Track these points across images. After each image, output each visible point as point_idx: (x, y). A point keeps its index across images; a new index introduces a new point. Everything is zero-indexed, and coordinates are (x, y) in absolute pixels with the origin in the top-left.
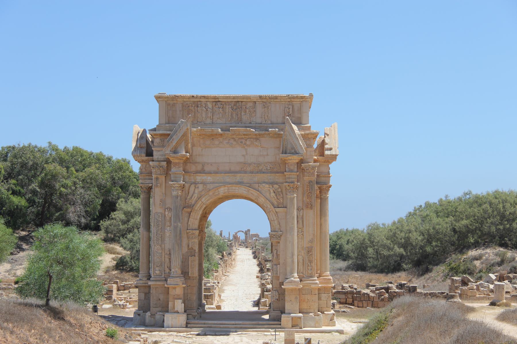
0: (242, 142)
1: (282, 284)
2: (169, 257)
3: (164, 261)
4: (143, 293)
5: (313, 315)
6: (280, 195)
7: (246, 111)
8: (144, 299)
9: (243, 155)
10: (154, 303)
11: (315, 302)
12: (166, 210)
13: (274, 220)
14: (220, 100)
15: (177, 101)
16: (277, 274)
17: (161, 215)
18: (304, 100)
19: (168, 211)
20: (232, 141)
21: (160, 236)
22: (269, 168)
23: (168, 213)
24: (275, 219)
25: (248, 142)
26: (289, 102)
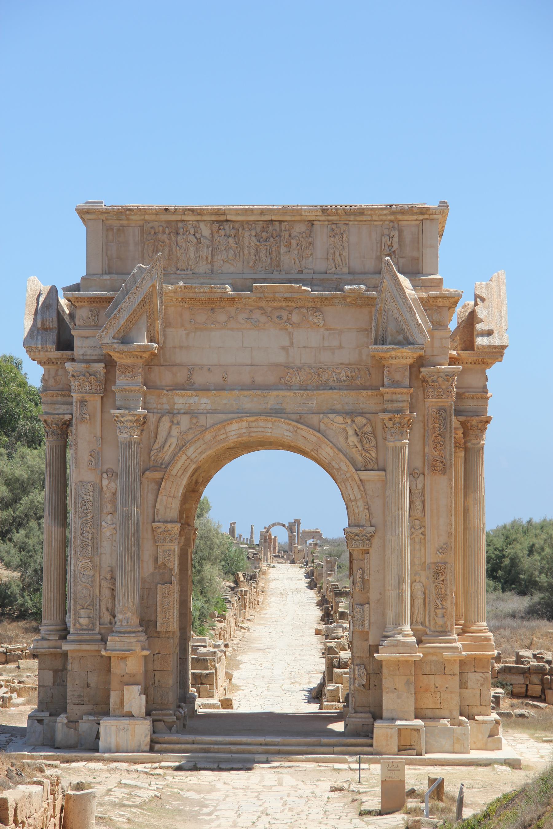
0: (280, 317)
1: (375, 649)
2: (110, 586)
3: (98, 594)
4: (49, 670)
5: (449, 724)
6: (369, 440)
7: (290, 243)
8: (50, 684)
9: (284, 348)
10: (76, 694)
11: (452, 692)
12: (105, 475)
13: (356, 500)
14: (229, 218)
15: (128, 219)
16: (363, 625)
17: (91, 488)
18: (426, 216)
19: (108, 478)
20: (257, 314)
21: (90, 536)
22: (344, 378)
23: (109, 483)
24: (359, 496)
25: (295, 318)
26: (391, 221)
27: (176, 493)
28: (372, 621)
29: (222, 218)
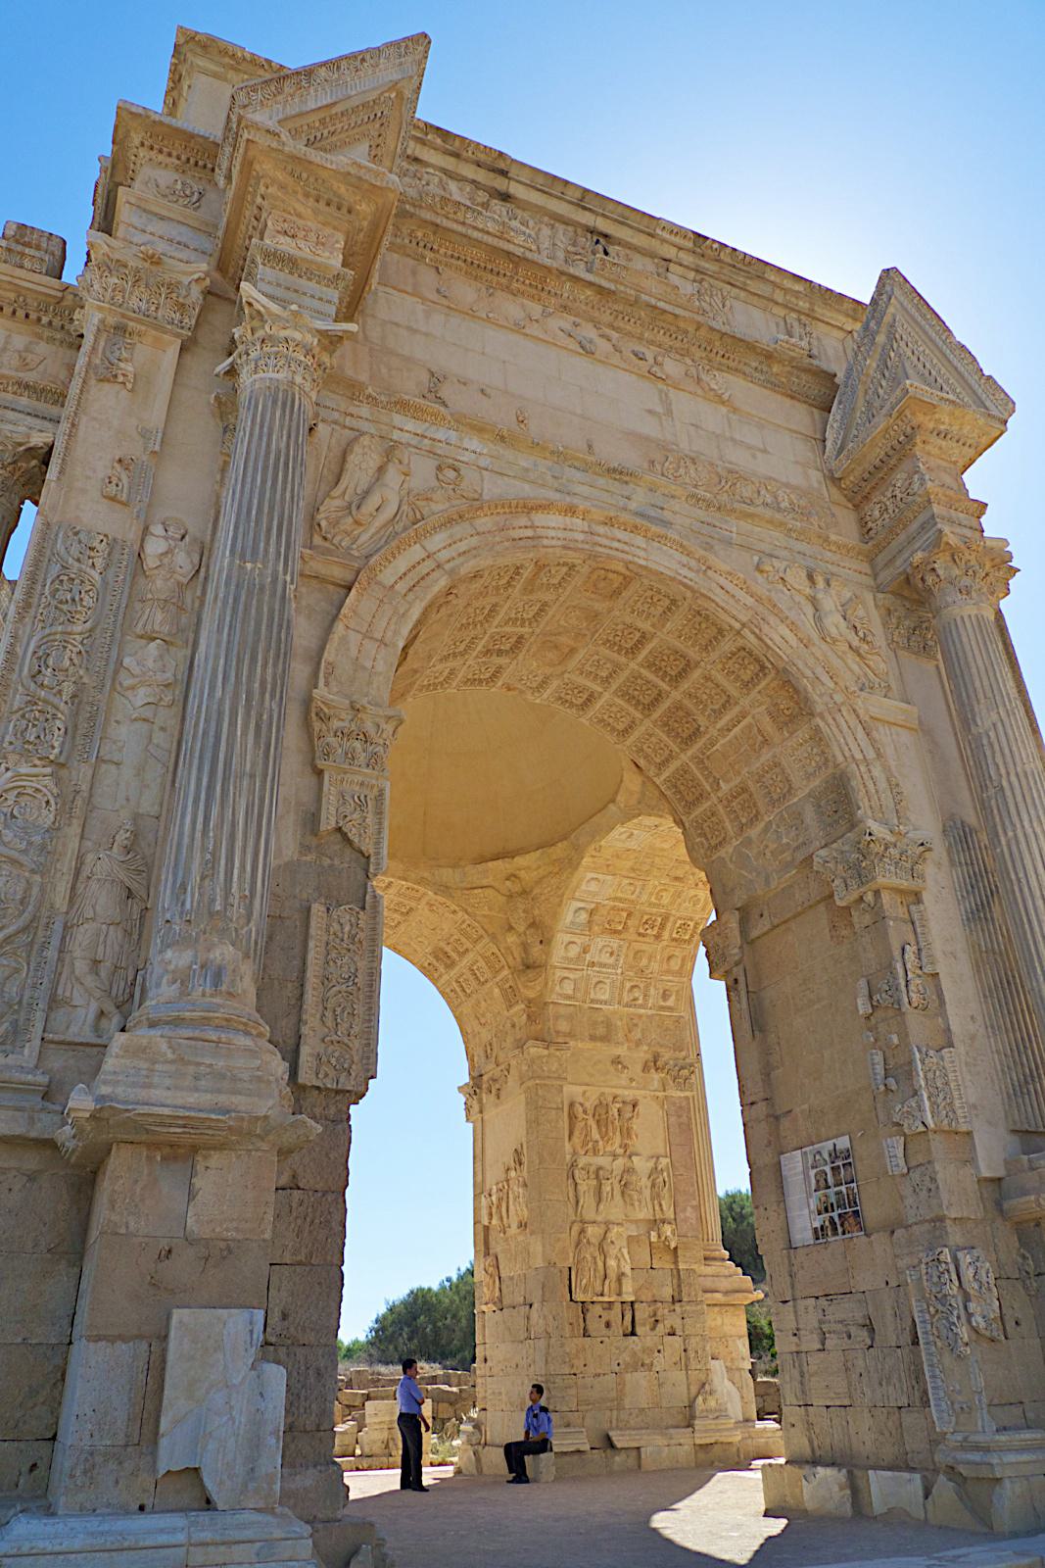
2: (122, 875)
3: (60, 901)
14: (515, 189)
21: (68, 689)
24: (871, 754)
25: (672, 367)
27: (389, 634)
29: (500, 184)
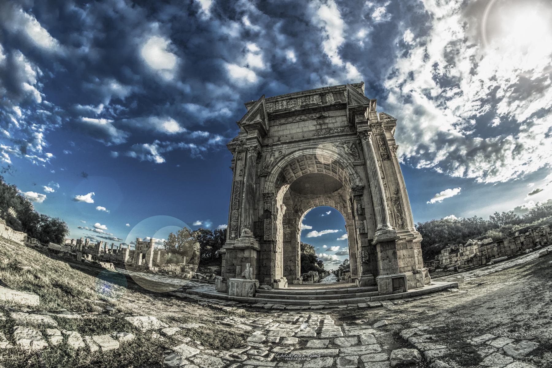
9: (314, 125)
10: (228, 268)
13: (353, 174)
16: (364, 229)
24: (354, 172)
28: (369, 228)
